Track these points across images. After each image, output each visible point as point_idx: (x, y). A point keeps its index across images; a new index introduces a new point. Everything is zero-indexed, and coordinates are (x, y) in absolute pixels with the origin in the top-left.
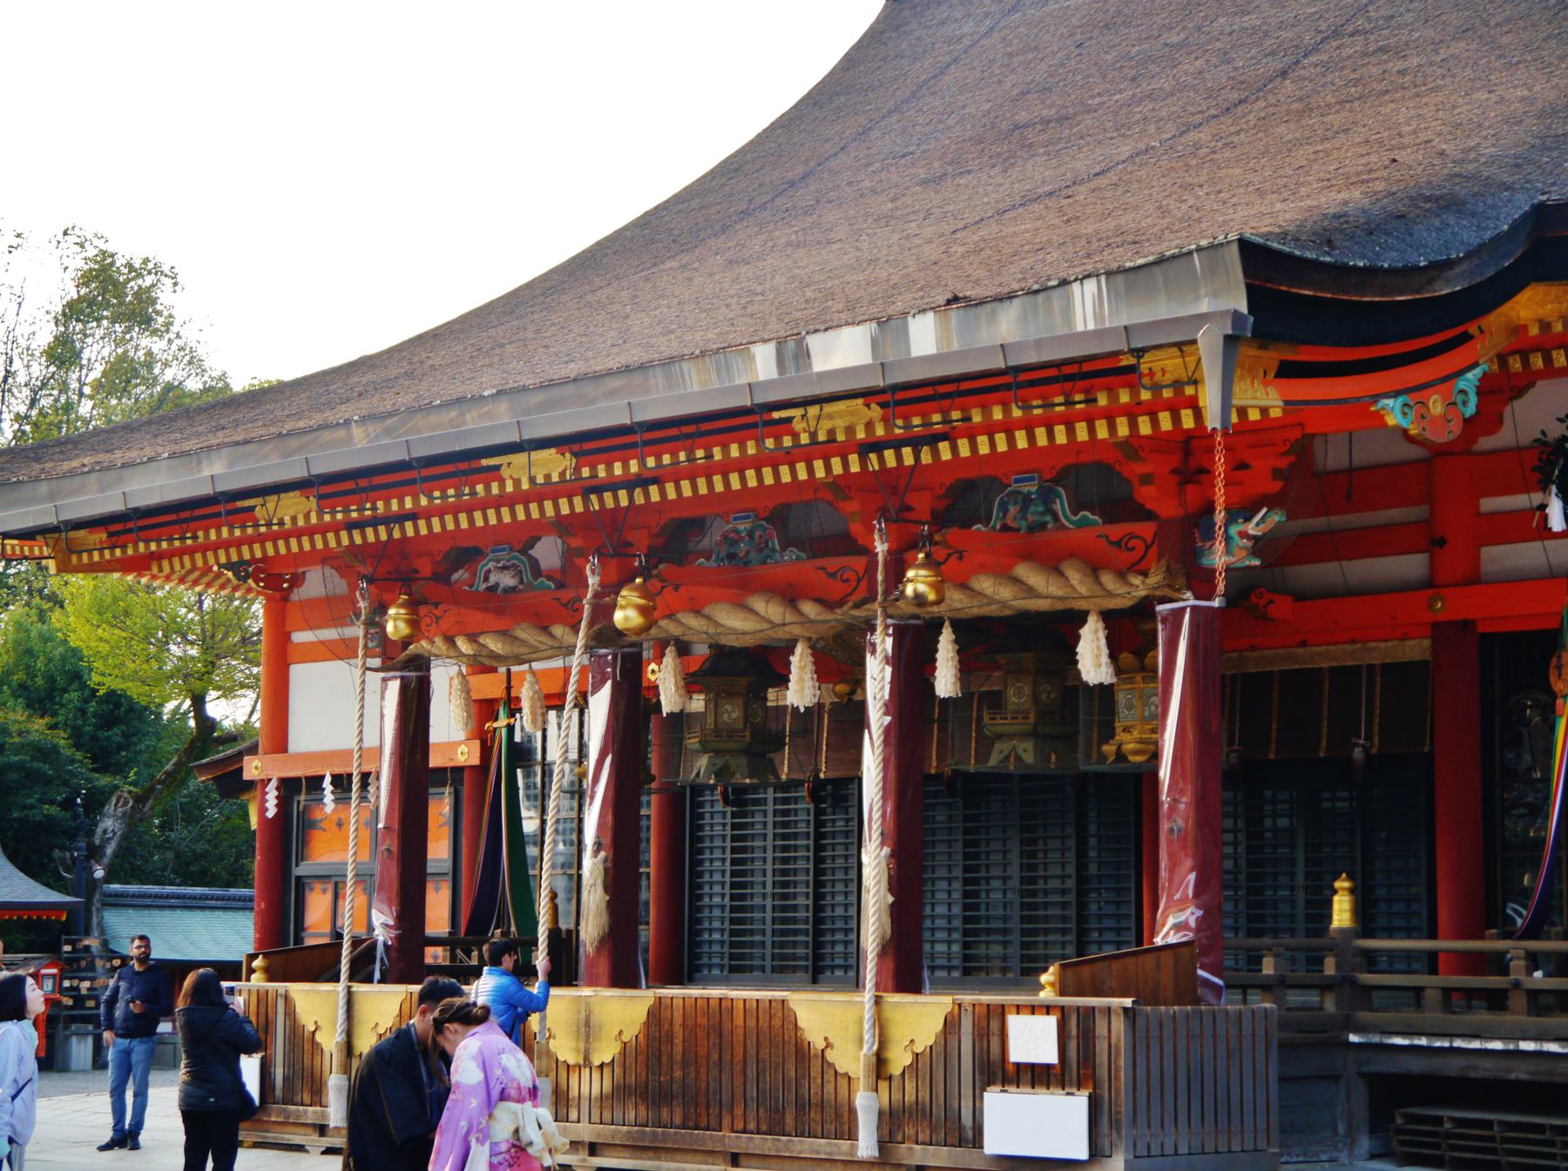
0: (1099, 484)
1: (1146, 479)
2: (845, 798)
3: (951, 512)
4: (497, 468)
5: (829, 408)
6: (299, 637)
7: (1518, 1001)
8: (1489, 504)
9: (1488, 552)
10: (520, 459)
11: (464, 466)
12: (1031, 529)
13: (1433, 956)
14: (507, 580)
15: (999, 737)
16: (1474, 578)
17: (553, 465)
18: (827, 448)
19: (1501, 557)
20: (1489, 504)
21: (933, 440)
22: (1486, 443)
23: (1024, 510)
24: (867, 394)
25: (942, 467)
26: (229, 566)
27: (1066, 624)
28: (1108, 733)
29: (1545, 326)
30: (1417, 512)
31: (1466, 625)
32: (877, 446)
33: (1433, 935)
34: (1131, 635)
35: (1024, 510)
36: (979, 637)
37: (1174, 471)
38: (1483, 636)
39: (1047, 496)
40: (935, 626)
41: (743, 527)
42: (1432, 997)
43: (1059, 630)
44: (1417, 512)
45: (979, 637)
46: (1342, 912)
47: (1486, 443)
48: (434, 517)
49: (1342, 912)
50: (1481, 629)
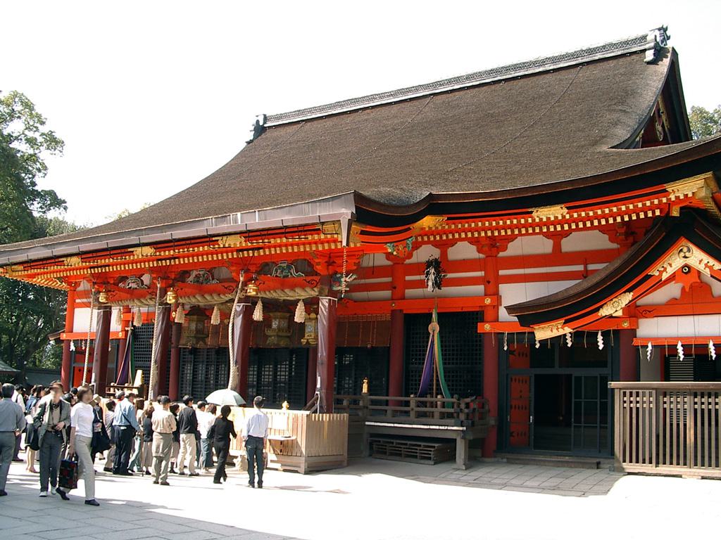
0: (305, 265)
1: (318, 264)
2: (225, 352)
3: (259, 269)
4: (133, 252)
5: (229, 237)
6: (78, 301)
7: (412, 414)
8: (408, 278)
9: (407, 291)
10: (139, 249)
11: (123, 251)
12: (284, 277)
13: (387, 401)
14: (134, 286)
15: (270, 336)
16: (403, 298)
17: (148, 251)
18: (228, 250)
19: (409, 292)
20: (408, 278)
21: (258, 249)
22: (407, 261)
23: (282, 271)
24: (241, 233)
25: (258, 259)
26: (58, 278)
27: (295, 303)
28: (303, 336)
29: (430, 228)
30: (389, 279)
31: (401, 311)
32: (242, 250)
33: (387, 395)
34: (311, 305)
35: (282, 271)
36: (269, 306)
37: (326, 262)
38: (405, 314)
39: (289, 267)
40: (255, 304)
41: (201, 273)
42: (389, 412)
43: (290, 307)
44: (389, 279)
45: (269, 306)
46: (365, 390)
47: (407, 261)
48: (113, 266)
49: (365, 390)
50: (404, 312)
